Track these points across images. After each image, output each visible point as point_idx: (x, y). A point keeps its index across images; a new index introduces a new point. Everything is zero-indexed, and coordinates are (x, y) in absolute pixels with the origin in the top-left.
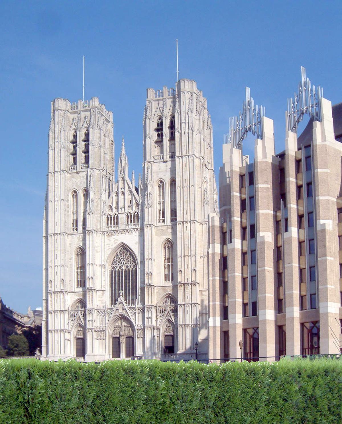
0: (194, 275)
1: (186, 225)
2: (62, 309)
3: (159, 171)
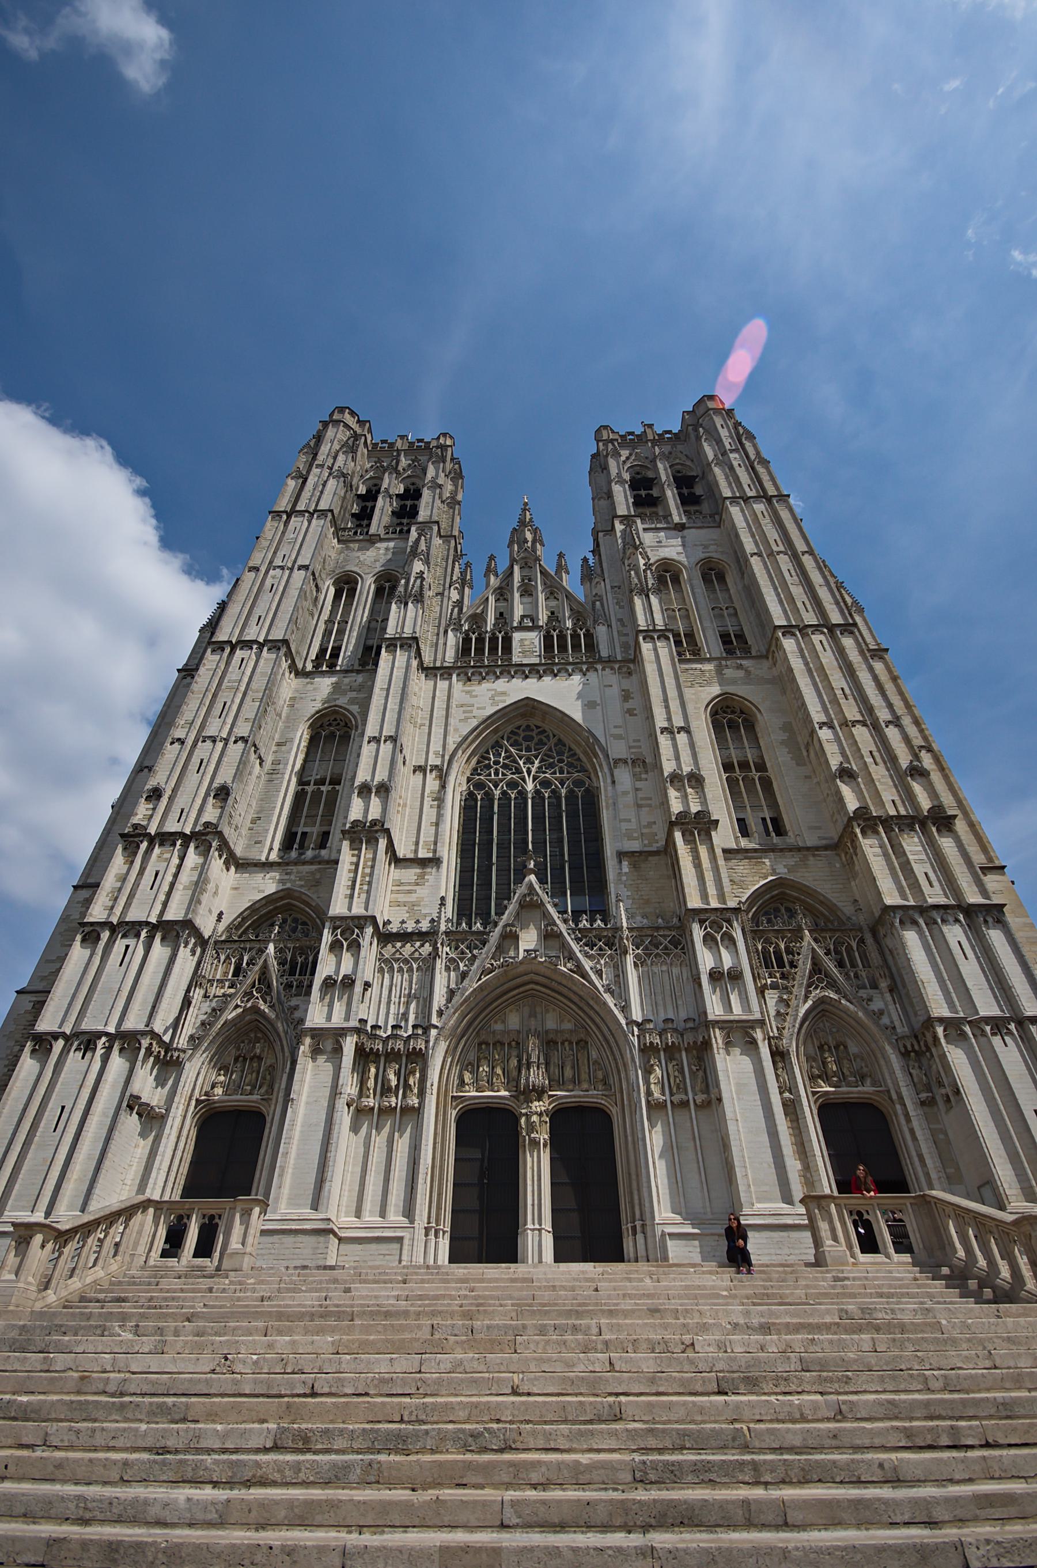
0: (917, 788)
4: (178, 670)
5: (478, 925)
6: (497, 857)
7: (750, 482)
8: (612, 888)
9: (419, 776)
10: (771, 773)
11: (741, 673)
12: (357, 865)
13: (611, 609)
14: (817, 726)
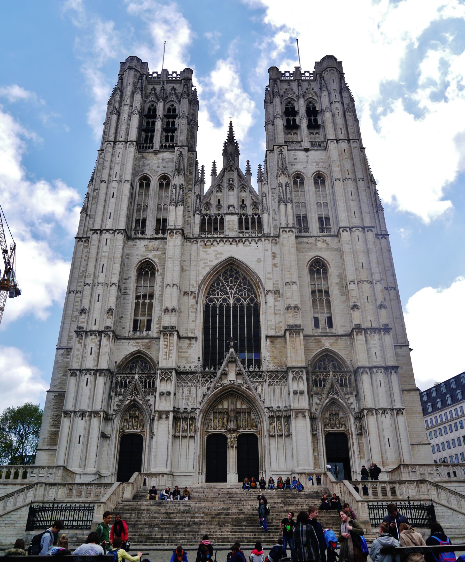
3: (294, 161)
4: (75, 238)
5: (212, 369)
6: (219, 335)
7: (342, 127)
9: (186, 297)
10: (331, 298)
11: (324, 245)
12: (167, 346)
13: (270, 204)
14: (348, 283)
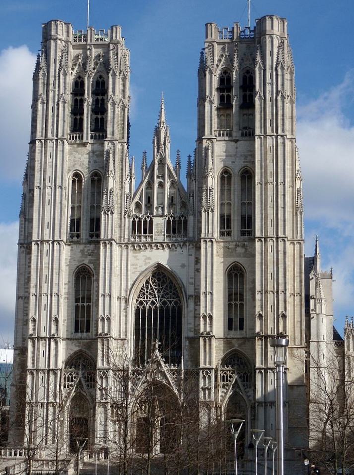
1: (270, 243)
2: (52, 367)
8: (183, 350)
10: (244, 302)
11: (243, 250)
